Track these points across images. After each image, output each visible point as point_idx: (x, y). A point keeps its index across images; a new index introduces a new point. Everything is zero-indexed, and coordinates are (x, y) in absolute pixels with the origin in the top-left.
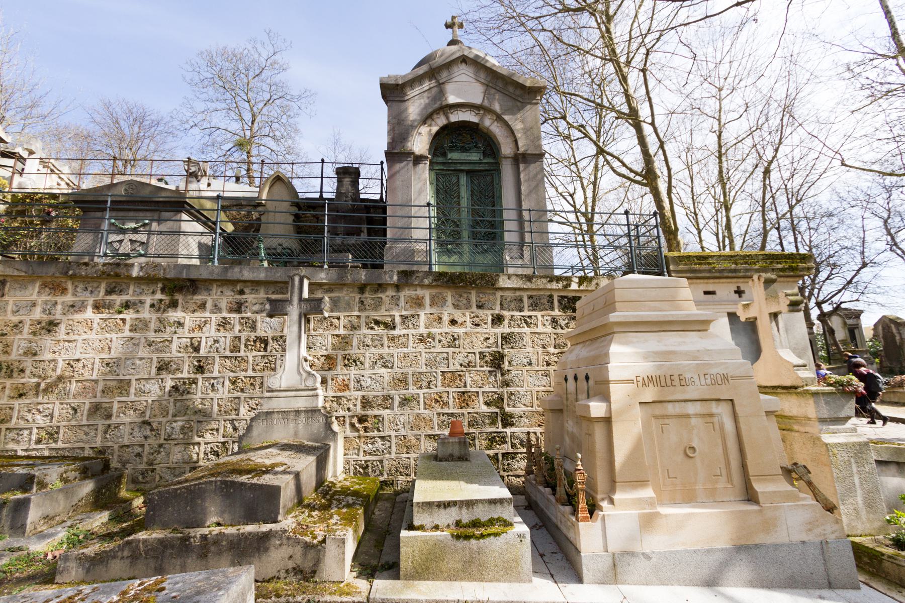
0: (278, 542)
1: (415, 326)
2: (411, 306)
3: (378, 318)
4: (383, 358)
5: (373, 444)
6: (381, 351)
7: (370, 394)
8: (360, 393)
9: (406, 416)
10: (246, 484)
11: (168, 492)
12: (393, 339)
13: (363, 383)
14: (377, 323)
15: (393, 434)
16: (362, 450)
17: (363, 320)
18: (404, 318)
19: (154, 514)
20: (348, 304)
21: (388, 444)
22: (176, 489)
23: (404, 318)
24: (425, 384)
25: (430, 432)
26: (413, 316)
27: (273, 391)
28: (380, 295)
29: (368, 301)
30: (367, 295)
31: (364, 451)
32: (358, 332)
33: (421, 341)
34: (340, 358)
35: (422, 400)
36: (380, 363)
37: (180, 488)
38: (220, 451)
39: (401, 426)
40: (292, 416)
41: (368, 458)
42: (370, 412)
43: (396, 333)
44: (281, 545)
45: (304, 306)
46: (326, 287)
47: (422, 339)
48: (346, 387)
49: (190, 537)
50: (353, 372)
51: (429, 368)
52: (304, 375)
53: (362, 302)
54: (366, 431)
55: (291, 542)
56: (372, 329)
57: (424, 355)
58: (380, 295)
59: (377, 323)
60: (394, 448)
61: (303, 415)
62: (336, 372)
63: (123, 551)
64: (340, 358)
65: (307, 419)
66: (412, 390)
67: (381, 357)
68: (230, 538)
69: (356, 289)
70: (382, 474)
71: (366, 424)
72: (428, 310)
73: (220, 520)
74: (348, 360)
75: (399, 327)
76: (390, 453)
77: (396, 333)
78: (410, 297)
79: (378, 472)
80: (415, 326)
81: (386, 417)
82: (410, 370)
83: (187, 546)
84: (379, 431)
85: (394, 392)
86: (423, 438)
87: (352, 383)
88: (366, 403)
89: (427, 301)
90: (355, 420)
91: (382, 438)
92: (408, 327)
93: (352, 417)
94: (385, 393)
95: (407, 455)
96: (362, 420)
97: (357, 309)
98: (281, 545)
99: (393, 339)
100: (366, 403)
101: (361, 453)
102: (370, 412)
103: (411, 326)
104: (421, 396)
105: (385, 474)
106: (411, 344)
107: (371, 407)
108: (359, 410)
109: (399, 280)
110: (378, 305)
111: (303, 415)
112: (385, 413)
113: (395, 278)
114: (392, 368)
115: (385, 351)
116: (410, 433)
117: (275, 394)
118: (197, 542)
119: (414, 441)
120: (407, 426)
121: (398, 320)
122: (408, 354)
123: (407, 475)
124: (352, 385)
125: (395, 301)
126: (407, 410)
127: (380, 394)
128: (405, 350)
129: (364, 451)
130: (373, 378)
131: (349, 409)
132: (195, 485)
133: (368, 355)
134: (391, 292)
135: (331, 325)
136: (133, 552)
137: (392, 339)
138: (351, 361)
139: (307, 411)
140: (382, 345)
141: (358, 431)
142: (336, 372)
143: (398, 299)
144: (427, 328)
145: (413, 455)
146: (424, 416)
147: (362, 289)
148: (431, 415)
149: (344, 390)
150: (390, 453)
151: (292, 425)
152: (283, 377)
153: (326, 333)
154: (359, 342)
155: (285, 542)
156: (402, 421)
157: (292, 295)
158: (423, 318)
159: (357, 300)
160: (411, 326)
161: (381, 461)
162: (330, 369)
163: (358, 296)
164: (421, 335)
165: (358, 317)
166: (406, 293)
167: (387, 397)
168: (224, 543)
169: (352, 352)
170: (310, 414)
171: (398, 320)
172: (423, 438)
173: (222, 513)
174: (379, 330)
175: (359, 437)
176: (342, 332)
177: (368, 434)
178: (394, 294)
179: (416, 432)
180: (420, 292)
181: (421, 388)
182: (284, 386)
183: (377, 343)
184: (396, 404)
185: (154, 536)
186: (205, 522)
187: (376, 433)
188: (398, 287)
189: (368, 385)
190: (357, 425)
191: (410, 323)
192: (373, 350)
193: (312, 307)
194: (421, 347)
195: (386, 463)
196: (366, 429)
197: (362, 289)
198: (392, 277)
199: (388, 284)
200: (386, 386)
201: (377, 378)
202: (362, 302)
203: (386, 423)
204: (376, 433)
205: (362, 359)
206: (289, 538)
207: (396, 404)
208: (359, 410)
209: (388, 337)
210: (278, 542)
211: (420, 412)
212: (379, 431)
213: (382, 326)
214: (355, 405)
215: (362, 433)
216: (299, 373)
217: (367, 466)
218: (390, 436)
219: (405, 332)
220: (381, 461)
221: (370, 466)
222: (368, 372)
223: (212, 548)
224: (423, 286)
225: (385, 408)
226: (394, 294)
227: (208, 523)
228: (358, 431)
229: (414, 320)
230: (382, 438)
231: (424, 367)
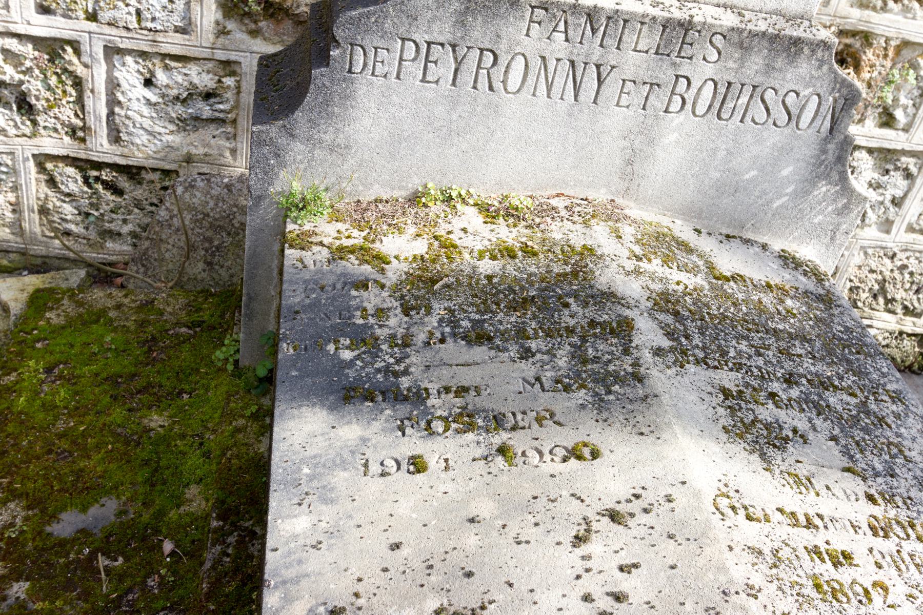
38: (34, 86)
40: (633, 60)
61: (704, 68)
76: (887, 225)
150: (887, 225)
151: (617, 117)
212: (888, 120)
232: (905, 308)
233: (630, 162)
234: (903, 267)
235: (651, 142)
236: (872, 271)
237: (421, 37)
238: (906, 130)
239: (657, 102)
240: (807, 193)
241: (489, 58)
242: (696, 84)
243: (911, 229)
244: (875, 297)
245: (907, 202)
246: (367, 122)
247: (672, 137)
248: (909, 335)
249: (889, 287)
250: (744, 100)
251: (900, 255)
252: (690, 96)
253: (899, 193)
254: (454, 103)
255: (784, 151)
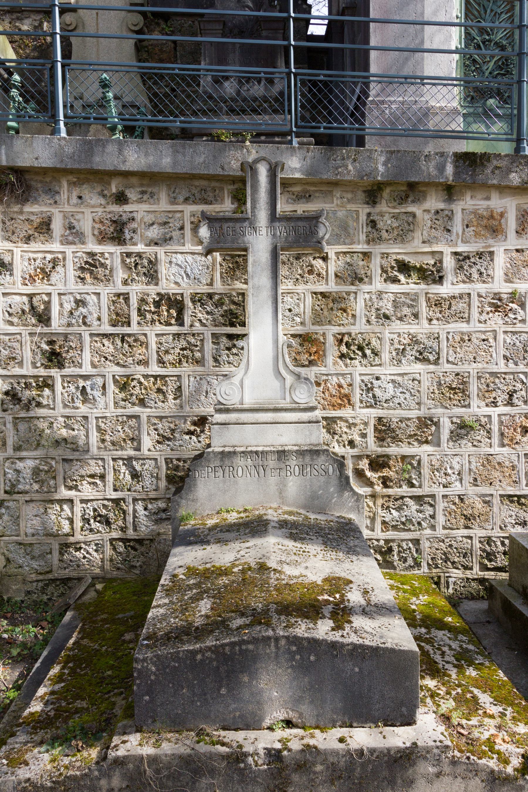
0: (431, 770)
1: (484, 277)
2: (477, 234)
3: (407, 259)
4: (417, 342)
5: (399, 509)
6: (414, 329)
7: (394, 415)
8: (374, 413)
9: (464, 455)
10: (343, 645)
11: (175, 657)
12: (438, 304)
13: (378, 392)
14: (404, 267)
15: (440, 491)
16: (378, 521)
17: (376, 263)
18: (461, 259)
19: (152, 701)
20: (345, 227)
21: (429, 511)
22: (194, 653)
23: (461, 259)
24: (503, 397)
25: (511, 491)
26: (480, 255)
27: (227, 411)
28: (411, 209)
29: (386, 222)
30: (383, 207)
31: (384, 523)
32: (366, 288)
33: (496, 308)
34: (330, 340)
35: (495, 428)
36: (411, 353)
37: (201, 650)
38: (111, 515)
39: (454, 477)
40: (272, 462)
41: (391, 534)
42: (393, 450)
43: (445, 289)
44: (438, 775)
45: (281, 229)
46: (297, 189)
47: (498, 304)
48: (346, 399)
49: (246, 755)
50: (359, 370)
51: (511, 364)
52: (289, 379)
53: (373, 224)
54: (386, 486)
55: (460, 769)
56: (395, 281)
57: (501, 337)
58: (411, 209)
59: (404, 267)
60: (441, 519)
61: (293, 462)
62: (323, 370)
63: (110, 777)
64: (330, 340)
65: (302, 468)
66: (478, 408)
67: (414, 341)
68: (331, 759)
69: (361, 195)
70: (418, 565)
71: (386, 472)
72: (513, 241)
73: (293, 716)
74: (348, 345)
75: (450, 277)
76: (433, 527)
77: (445, 289)
78: (475, 213)
79: (410, 561)
80: (484, 277)
81: (425, 460)
82: (473, 369)
83: (241, 772)
84: (412, 486)
85: (440, 410)
86: (496, 501)
87: (358, 391)
88: (385, 431)
89: (511, 223)
90: (364, 464)
91: (418, 499)
92: (469, 279)
93: (359, 457)
94: (423, 412)
95: (466, 532)
96: (378, 463)
97: (363, 237)
98: (438, 775)
99: (438, 304)
100: (385, 431)
101: (378, 526)
102: (393, 450)
103: (475, 276)
104: (495, 420)
105: (424, 564)
106: (475, 312)
107: (396, 439)
108: (372, 446)
109: (456, 174)
110: (405, 230)
111: (293, 462)
112: (424, 451)
113: (450, 169)
114: (436, 362)
115: (421, 329)
116: (471, 491)
117: (233, 417)
118: (259, 764)
119: (479, 505)
120: (467, 478)
121: (449, 263)
122: (469, 334)
123: (466, 568)
124: (357, 396)
125: (443, 221)
126: (466, 447)
127: (413, 414)
128: (463, 327)
129: (384, 523)
130: (397, 382)
131: (351, 443)
132: (232, 644)
133: (387, 336)
134: (434, 202)
135: (311, 272)
136: (131, 779)
137: (437, 303)
138: (354, 348)
139: (301, 453)
140: (416, 316)
141: (371, 484)
142: (323, 370)
143: (450, 218)
144: (508, 281)
145: (478, 533)
146: (499, 458)
147: (373, 193)
148: (514, 458)
149: (340, 406)
150: (433, 527)
151: (273, 480)
152: (246, 383)
153: (301, 288)
154: (368, 307)
155: (447, 769)
156: (457, 467)
157: (254, 207)
158: (501, 261)
159: (363, 218)
160: (475, 276)
161: (416, 542)
162: (311, 363)
163: (364, 211)
164: (497, 296)
165: (366, 255)
166: (468, 203)
167: (427, 423)
168: (319, 768)
169: (354, 330)
170: (308, 459)
171: (449, 263)
172: (496, 501)
173: (296, 702)
174: (409, 285)
175: (373, 496)
176: (331, 286)
177: (390, 491)
178: (441, 205)
179: (485, 490)
180: (497, 203)
181: (494, 404)
182: (249, 401)
183: (406, 311)
184: (445, 434)
185: (167, 748)
186: (261, 719)
187: (405, 490)
188: (450, 192)
189: (387, 396)
190: (368, 474)
191: (474, 270)
192: (397, 326)
193: (301, 238)
194: (496, 321)
195: (425, 545)
196: (385, 482)
197: (373, 193)
198: (441, 169)
199: (428, 184)
200: (425, 399)
201: (406, 381)
202: (373, 224)
203: (426, 471)
204: (405, 490)
205: (374, 342)
206: (454, 762)
207: (445, 434)
208: (372, 446)
209: (428, 300)
210: (431, 770)
211: (491, 451)
212: (412, 486)
213: (415, 276)
214: (364, 436)
215: (379, 488)
216: (278, 373)
217: (390, 550)
218: (433, 496)
219: (462, 288)
220: (416, 542)
221: (396, 549)
222: (388, 371)
223: (295, 777)
224: (505, 189)
225: (421, 443)
226: (441, 205)
227: (267, 722)
228: (371, 484)
229: (482, 265)
230: (418, 499)
231: (502, 362)
232: (462, 566)
233: (280, 493)
234: (451, 546)
235: (285, 486)
236: (437, 549)
237: (212, 466)
238: (420, 487)
239: (283, 474)
240: (342, 496)
241: (231, 469)
242: (293, 467)
243: (444, 528)
244: (446, 562)
245: (437, 516)
246: (201, 491)
247: (291, 484)
248: (473, 580)
249: (450, 556)
250: (309, 469)
251: (446, 540)
252: (292, 470)
253: (431, 513)
254: (224, 482)
255: (327, 483)
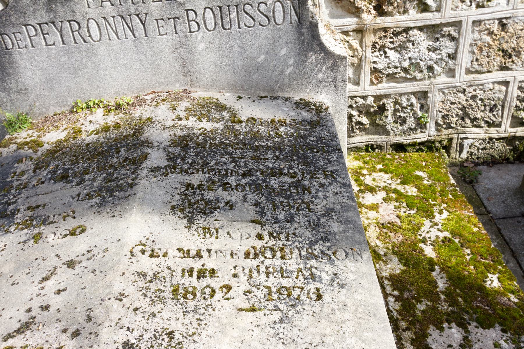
5: (400, 48)
21: (448, 46)
31: (375, 71)
41: (385, 87)
60: (465, 59)
70: (421, 125)
76: (451, 73)
79: (411, 122)
91: (433, 30)
95: (501, 76)
101: (366, 76)
129: (375, 71)
150: (451, 73)
161: (423, 95)
175: (360, 31)
177: (387, 21)
187: (413, 17)
195: (436, 99)
217: (382, 109)
218: (457, 24)
220: (423, 95)
221: (390, 104)
230: (433, 30)
232: (486, 122)
233: (184, 66)
234: (474, 97)
235: (190, 51)
236: (452, 103)
237: (34, 22)
238: (438, 10)
239: (182, 27)
240: (304, 62)
241: (76, 26)
242: (200, 12)
243: (468, 72)
244: (463, 119)
245: (459, 56)
246: (29, 74)
247: (202, 46)
248: (498, 139)
249: (470, 111)
250: (234, 15)
251: (468, 90)
252: (200, 19)
253: (451, 51)
254: (69, 53)
255: (275, 40)
